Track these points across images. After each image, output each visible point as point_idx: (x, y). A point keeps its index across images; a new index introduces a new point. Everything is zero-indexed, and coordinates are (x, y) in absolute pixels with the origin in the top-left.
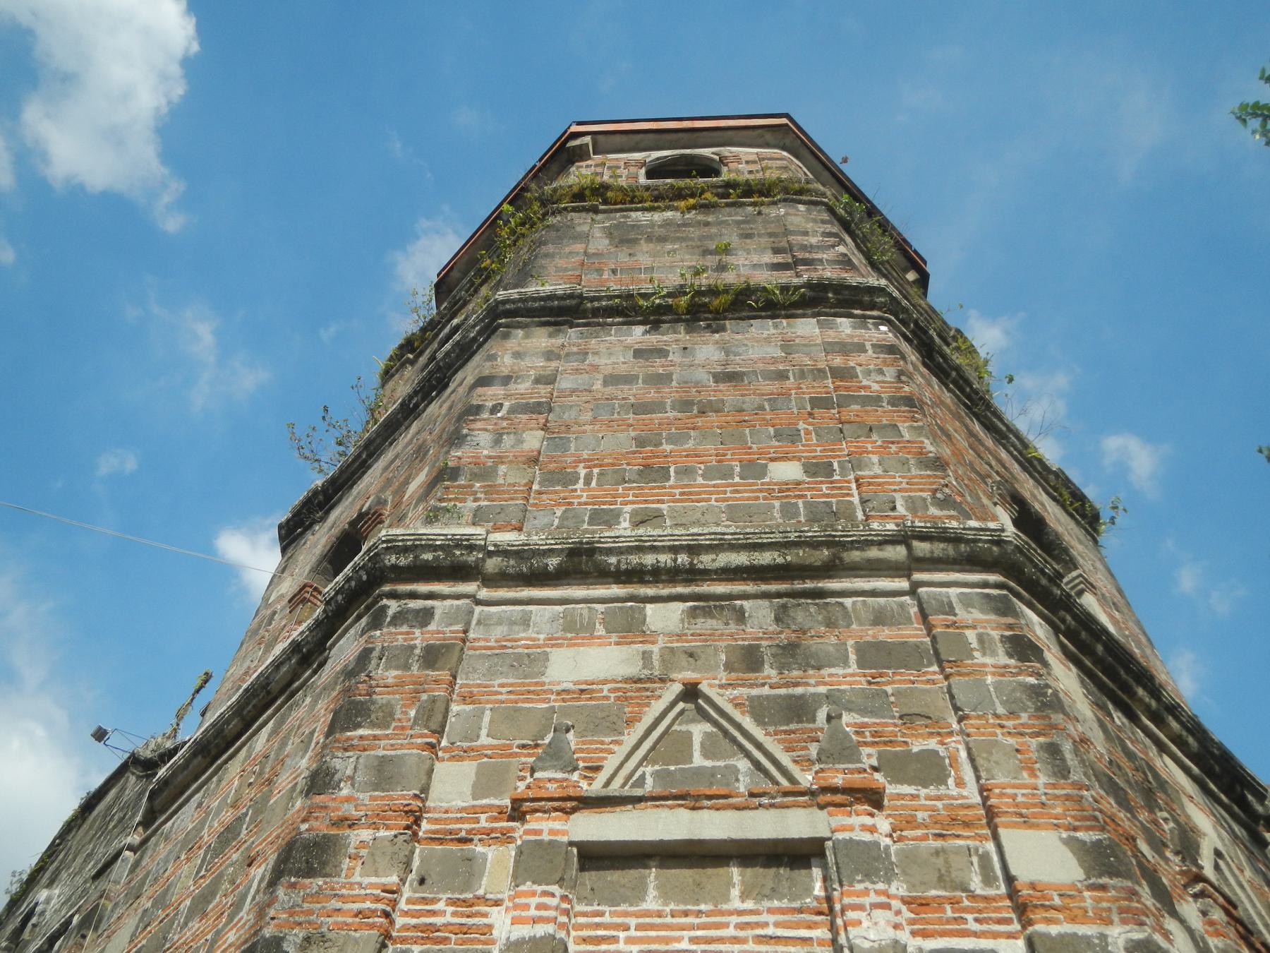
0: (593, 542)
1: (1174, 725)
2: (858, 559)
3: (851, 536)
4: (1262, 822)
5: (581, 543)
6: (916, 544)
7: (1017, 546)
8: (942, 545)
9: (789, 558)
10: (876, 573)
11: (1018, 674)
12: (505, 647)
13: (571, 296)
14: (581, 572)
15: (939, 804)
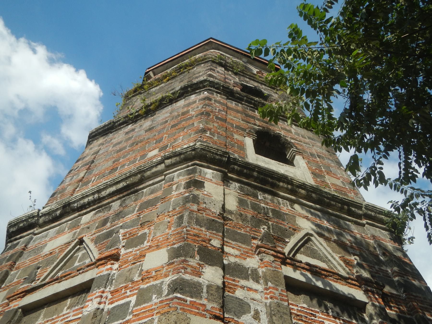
0: (69, 201)
1: (303, 192)
2: (149, 174)
3: (146, 167)
4: (363, 217)
5: (66, 203)
6: (166, 161)
7: (201, 149)
8: (175, 158)
9: (128, 183)
10: (156, 177)
11: (184, 194)
12: (37, 246)
13: (110, 123)
14: (67, 213)
15: (138, 252)
